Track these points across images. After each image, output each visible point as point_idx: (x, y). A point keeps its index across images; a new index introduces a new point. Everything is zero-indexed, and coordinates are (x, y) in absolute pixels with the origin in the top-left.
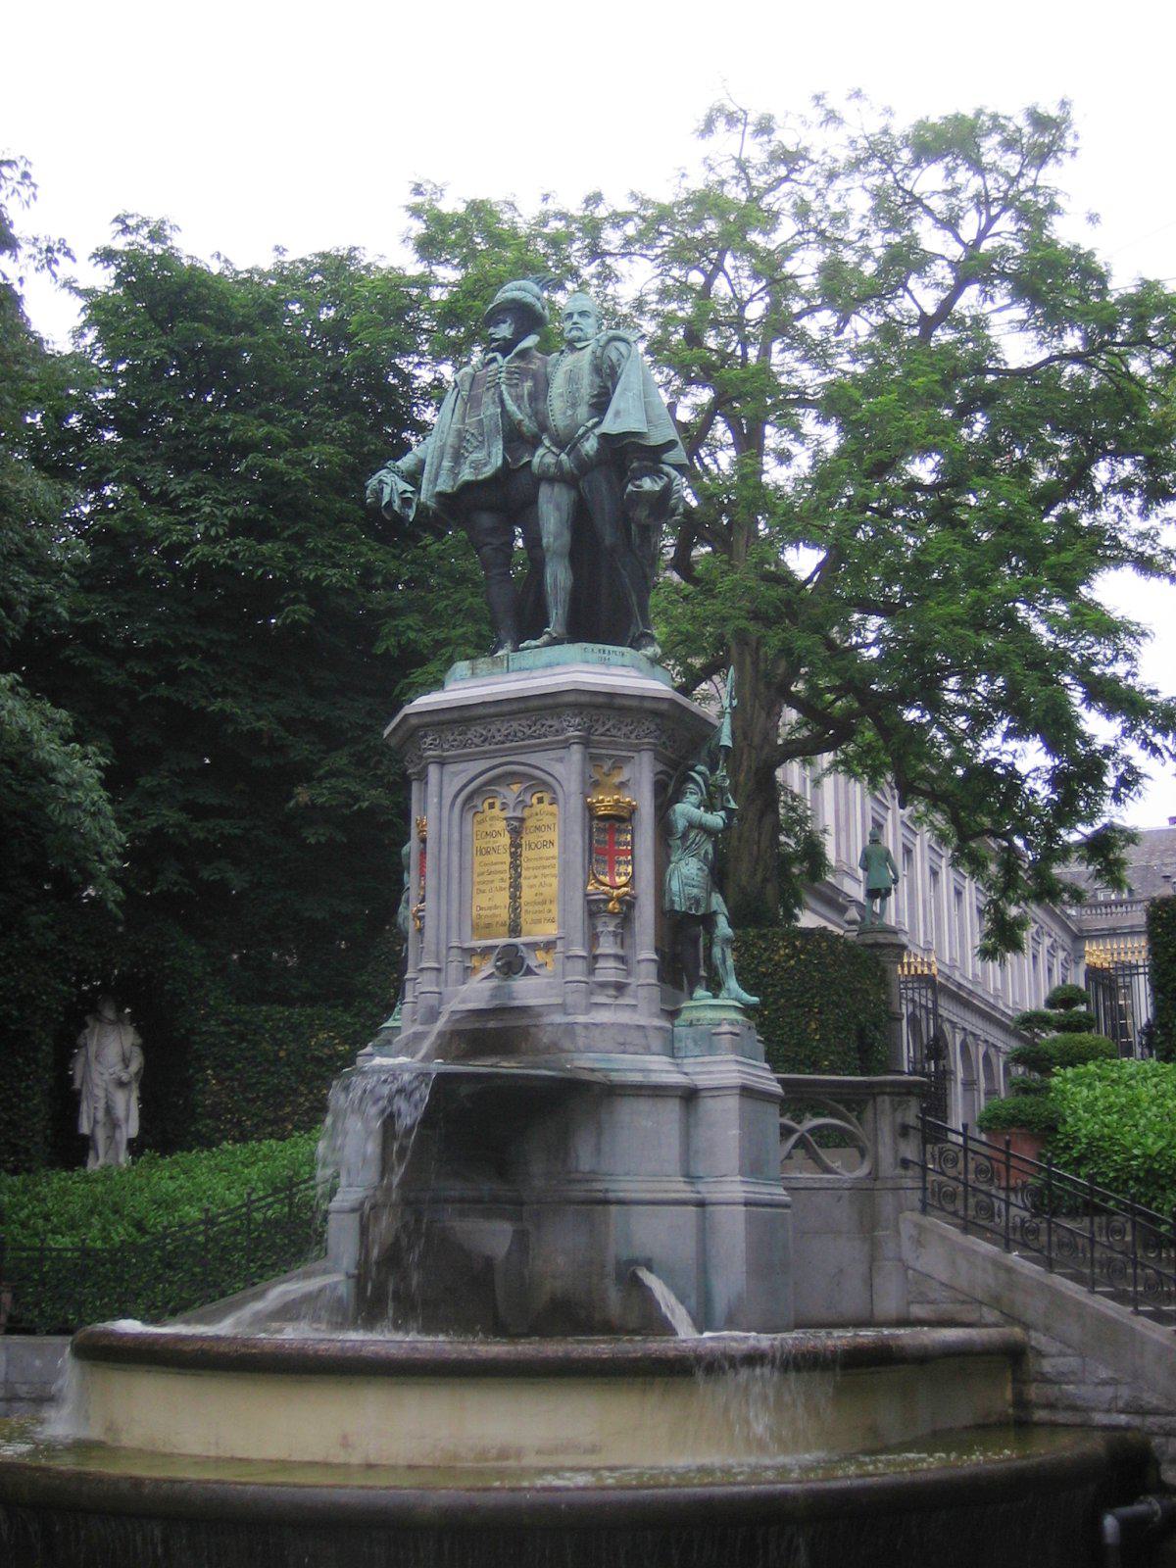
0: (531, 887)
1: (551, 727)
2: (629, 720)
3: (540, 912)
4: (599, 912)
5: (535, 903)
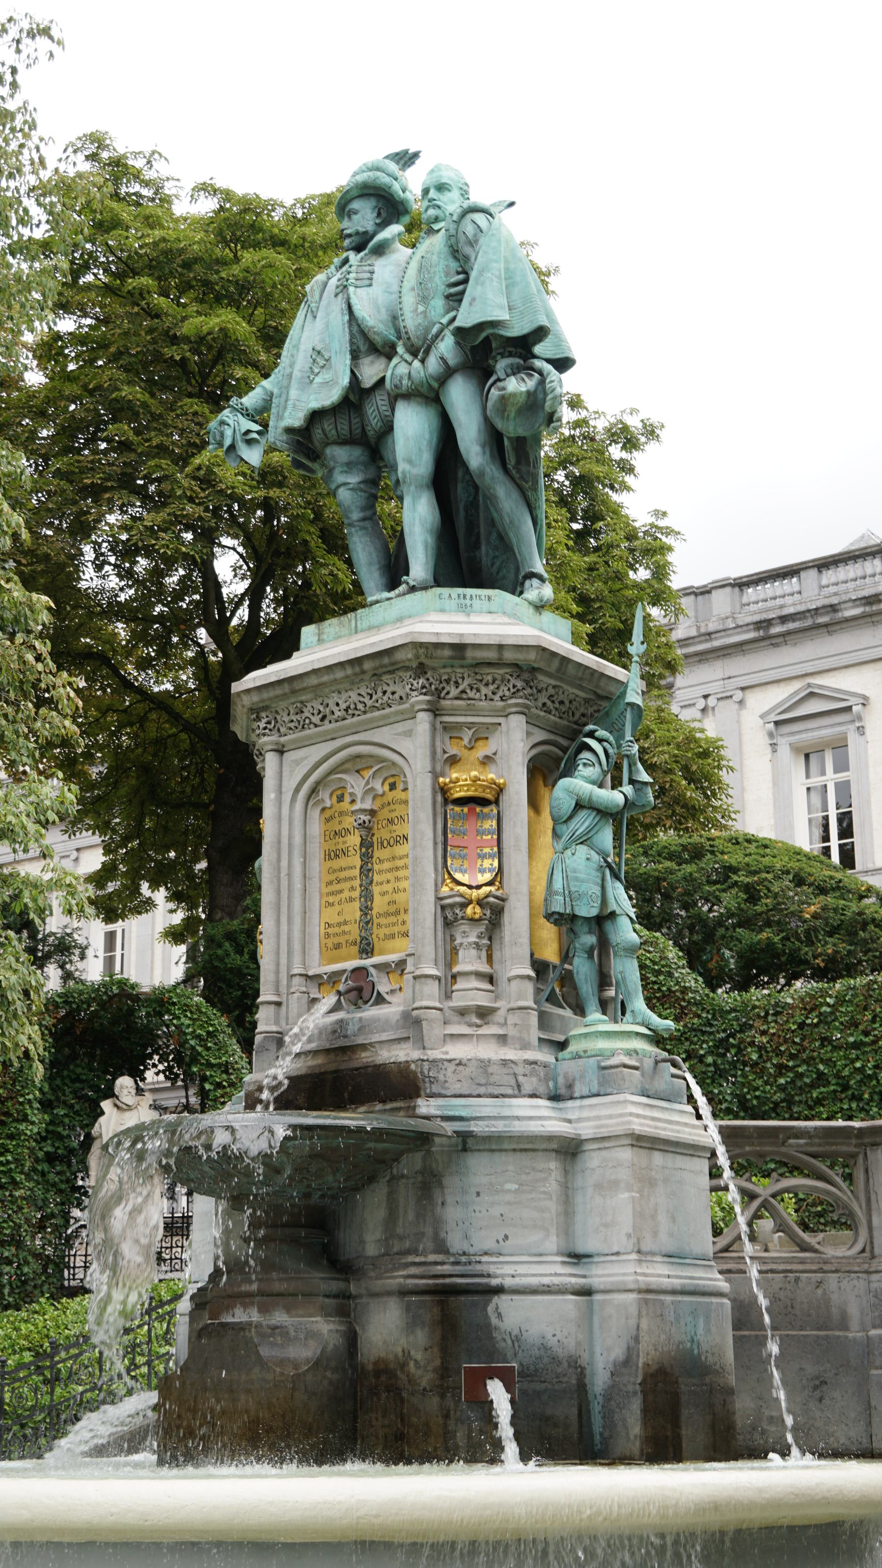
0: (383, 894)
1: (393, 693)
2: (490, 678)
3: (394, 924)
4: (456, 920)
5: (388, 914)
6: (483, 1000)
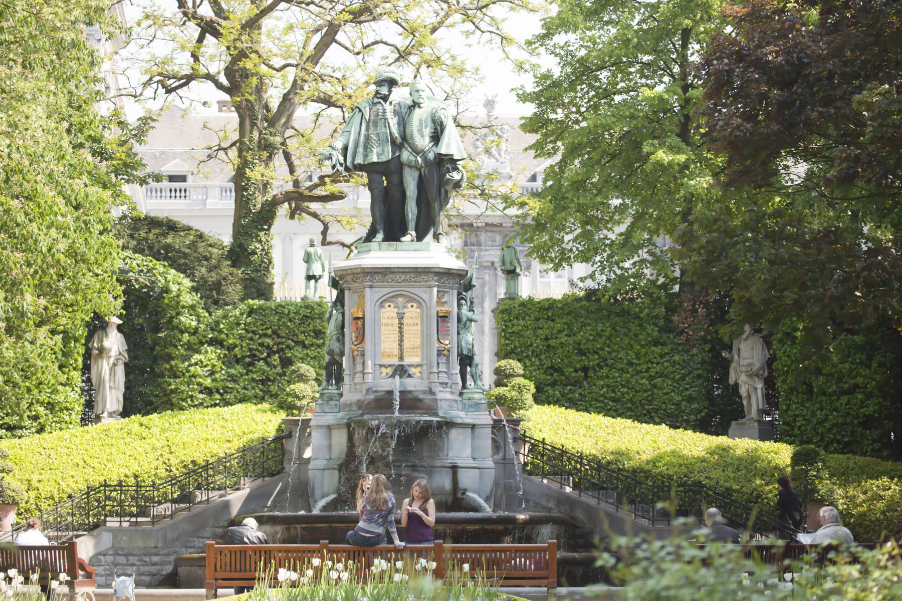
6: (447, 381)
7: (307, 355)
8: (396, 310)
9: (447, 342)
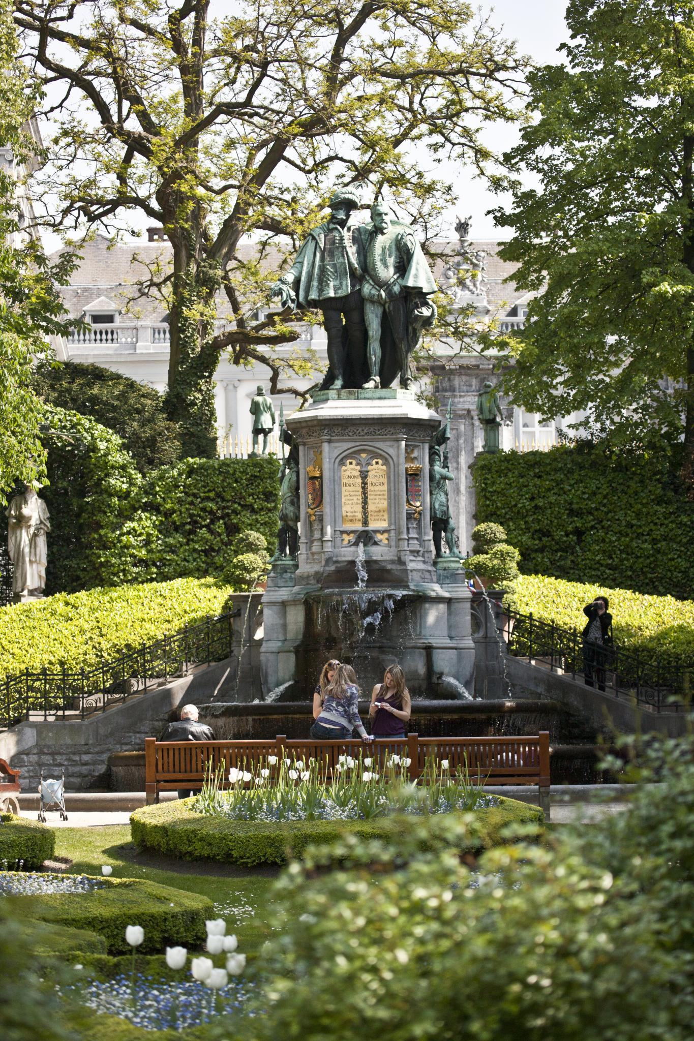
7: (257, 520)
8: (358, 468)
9: (418, 504)
